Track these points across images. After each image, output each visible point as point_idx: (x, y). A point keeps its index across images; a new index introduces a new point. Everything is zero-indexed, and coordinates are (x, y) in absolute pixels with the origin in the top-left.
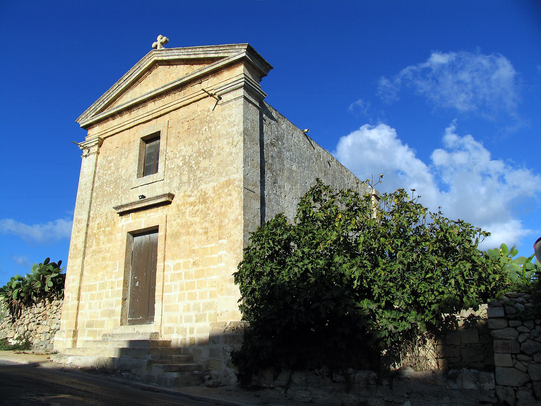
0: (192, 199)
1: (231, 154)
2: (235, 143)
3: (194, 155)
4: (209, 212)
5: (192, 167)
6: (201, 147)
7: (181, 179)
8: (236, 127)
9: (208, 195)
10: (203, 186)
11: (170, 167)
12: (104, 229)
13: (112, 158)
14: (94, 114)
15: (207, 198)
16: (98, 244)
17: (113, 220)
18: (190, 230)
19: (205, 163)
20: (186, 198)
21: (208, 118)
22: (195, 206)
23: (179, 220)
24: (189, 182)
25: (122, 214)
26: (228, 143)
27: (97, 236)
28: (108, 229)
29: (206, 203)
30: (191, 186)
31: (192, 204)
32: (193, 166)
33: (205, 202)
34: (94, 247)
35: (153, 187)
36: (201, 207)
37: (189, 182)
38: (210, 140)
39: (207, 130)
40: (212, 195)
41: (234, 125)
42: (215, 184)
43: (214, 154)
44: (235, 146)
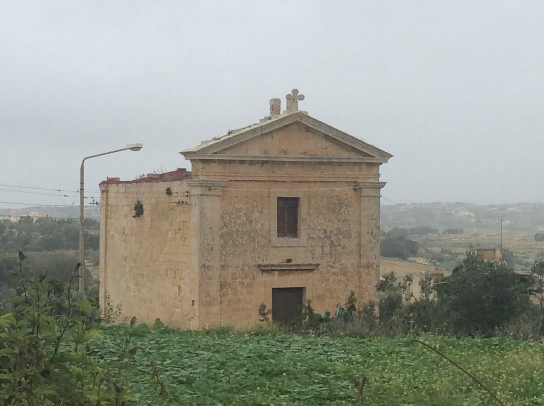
0: (334, 270)
1: (370, 242)
2: (374, 234)
3: (335, 232)
4: (349, 283)
5: (333, 241)
6: (341, 226)
7: (323, 250)
8: (374, 221)
9: (348, 270)
10: (343, 261)
11: (311, 236)
12: (241, 280)
13: (240, 206)
14: (218, 150)
15: (348, 272)
16: (236, 294)
17: (252, 273)
18: (334, 295)
19: (344, 242)
20: (329, 268)
21: (346, 201)
22: (337, 276)
23: (324, 285)
24: (331, 254)
25: (263, 271)
26: (368, 233)
27: (232, 286)
28: (246, 281)
29: (346, 276)
30: (333, 259)
31: (334, 274)
32: (335, 241)
33: (345, 274)
34: (230, 296)
35: (297, 250)
36: (343, 278)
37: (331, 254)
38: (349, 223)
39: (346, 212)
40: (352, 270)
41: (373, 219)
42: (354, 262)
43: (353, 236)
44: (374, 237)
